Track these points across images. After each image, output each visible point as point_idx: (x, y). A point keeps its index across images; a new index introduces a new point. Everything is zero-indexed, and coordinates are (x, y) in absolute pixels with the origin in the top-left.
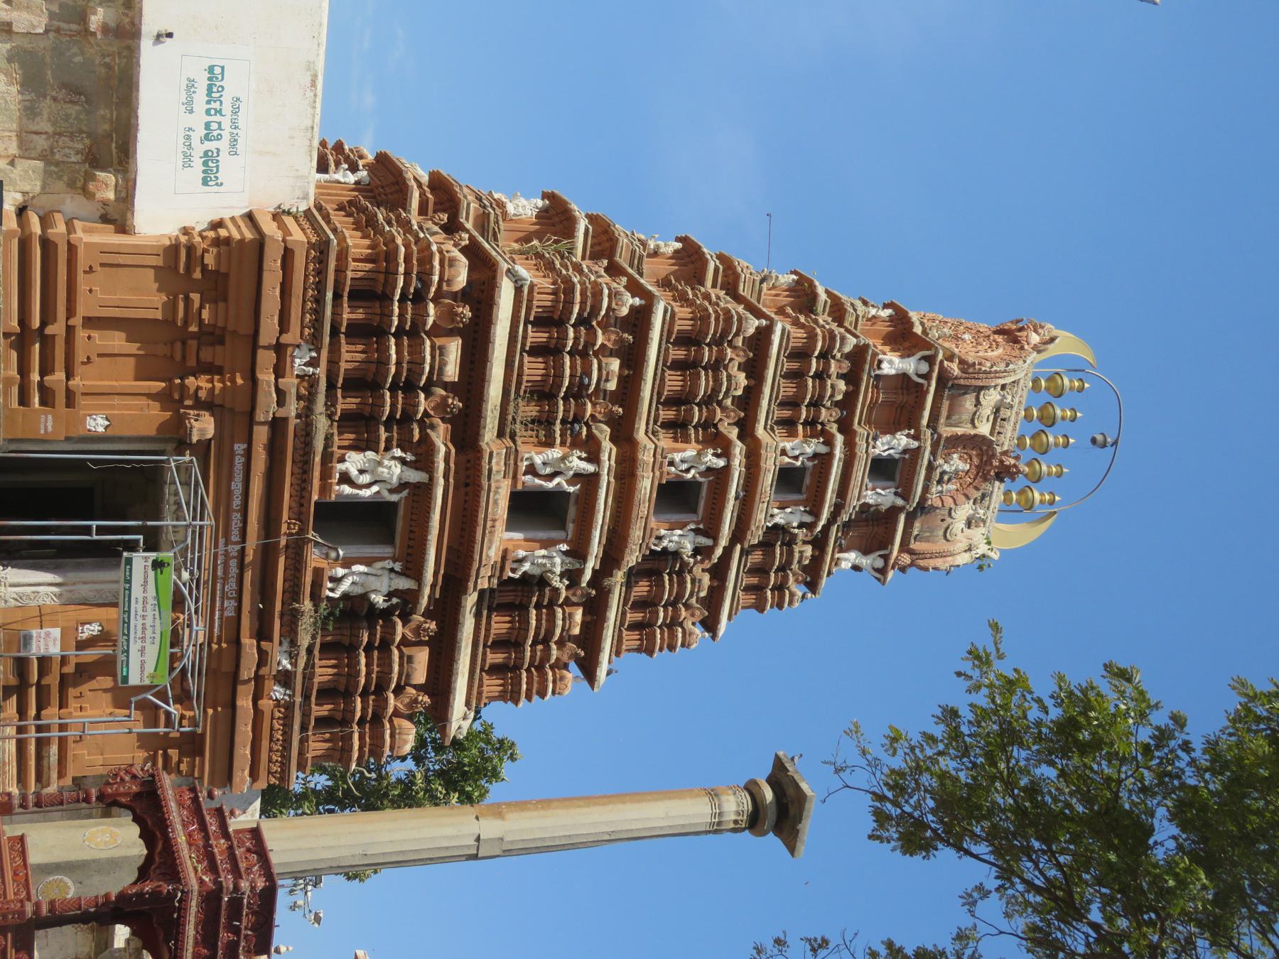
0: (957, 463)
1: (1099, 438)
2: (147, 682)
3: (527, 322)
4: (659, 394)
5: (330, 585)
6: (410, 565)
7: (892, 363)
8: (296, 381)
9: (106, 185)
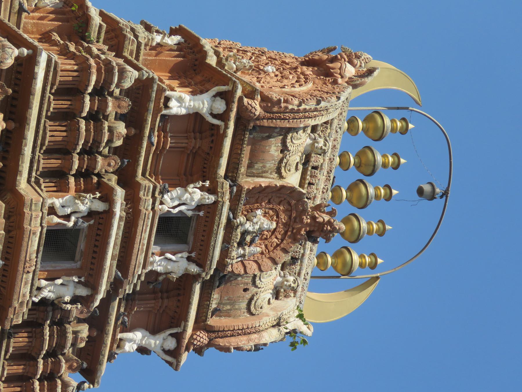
0: (261, 221)
1: (427, 188)
7: (182, 102)
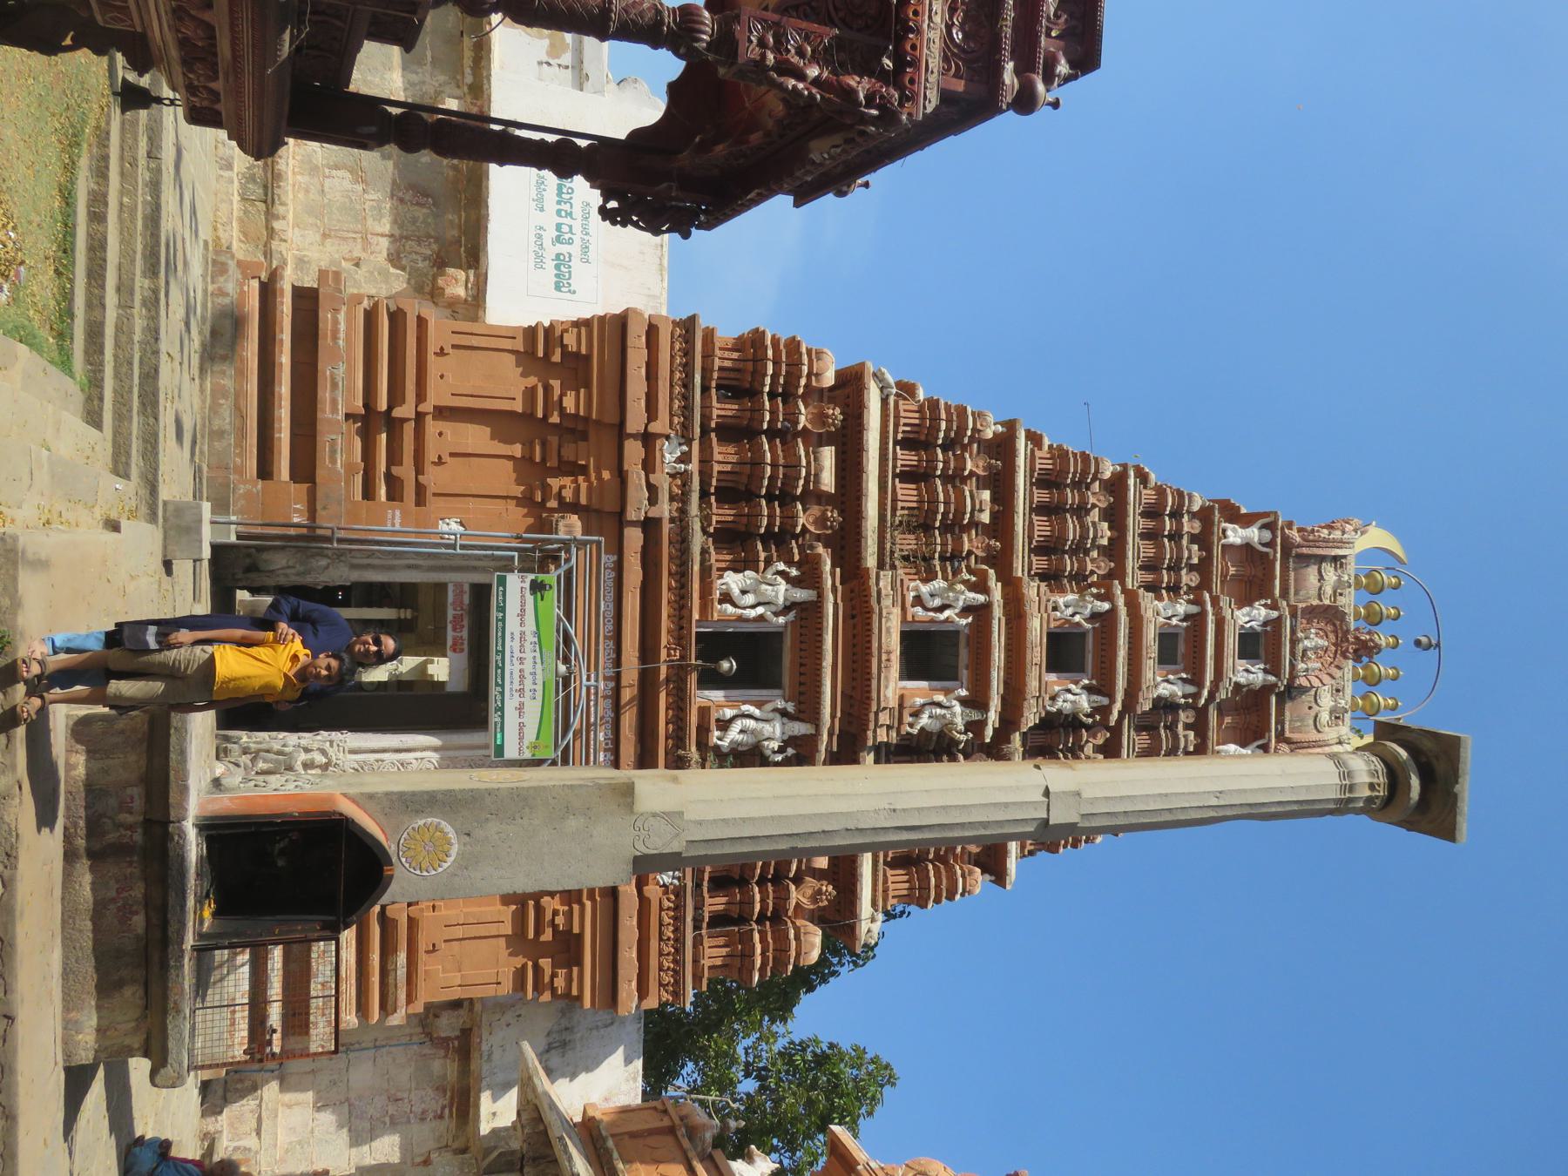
1: (1424, 640)
2: (527, 755)
3: (896, 443)
4: (1031, 538)
5: (717, 733)
6: (803, 707)
7: (1236, 535)
8: (669, 479)
9: (456, 284)
